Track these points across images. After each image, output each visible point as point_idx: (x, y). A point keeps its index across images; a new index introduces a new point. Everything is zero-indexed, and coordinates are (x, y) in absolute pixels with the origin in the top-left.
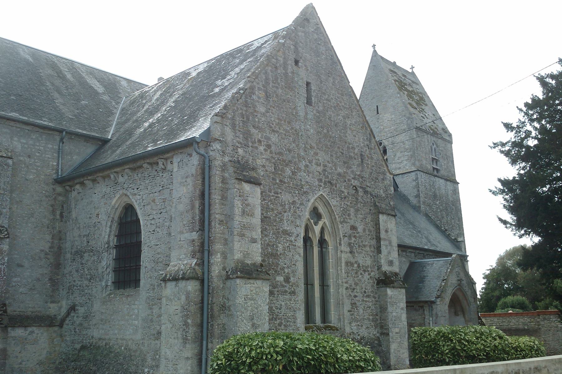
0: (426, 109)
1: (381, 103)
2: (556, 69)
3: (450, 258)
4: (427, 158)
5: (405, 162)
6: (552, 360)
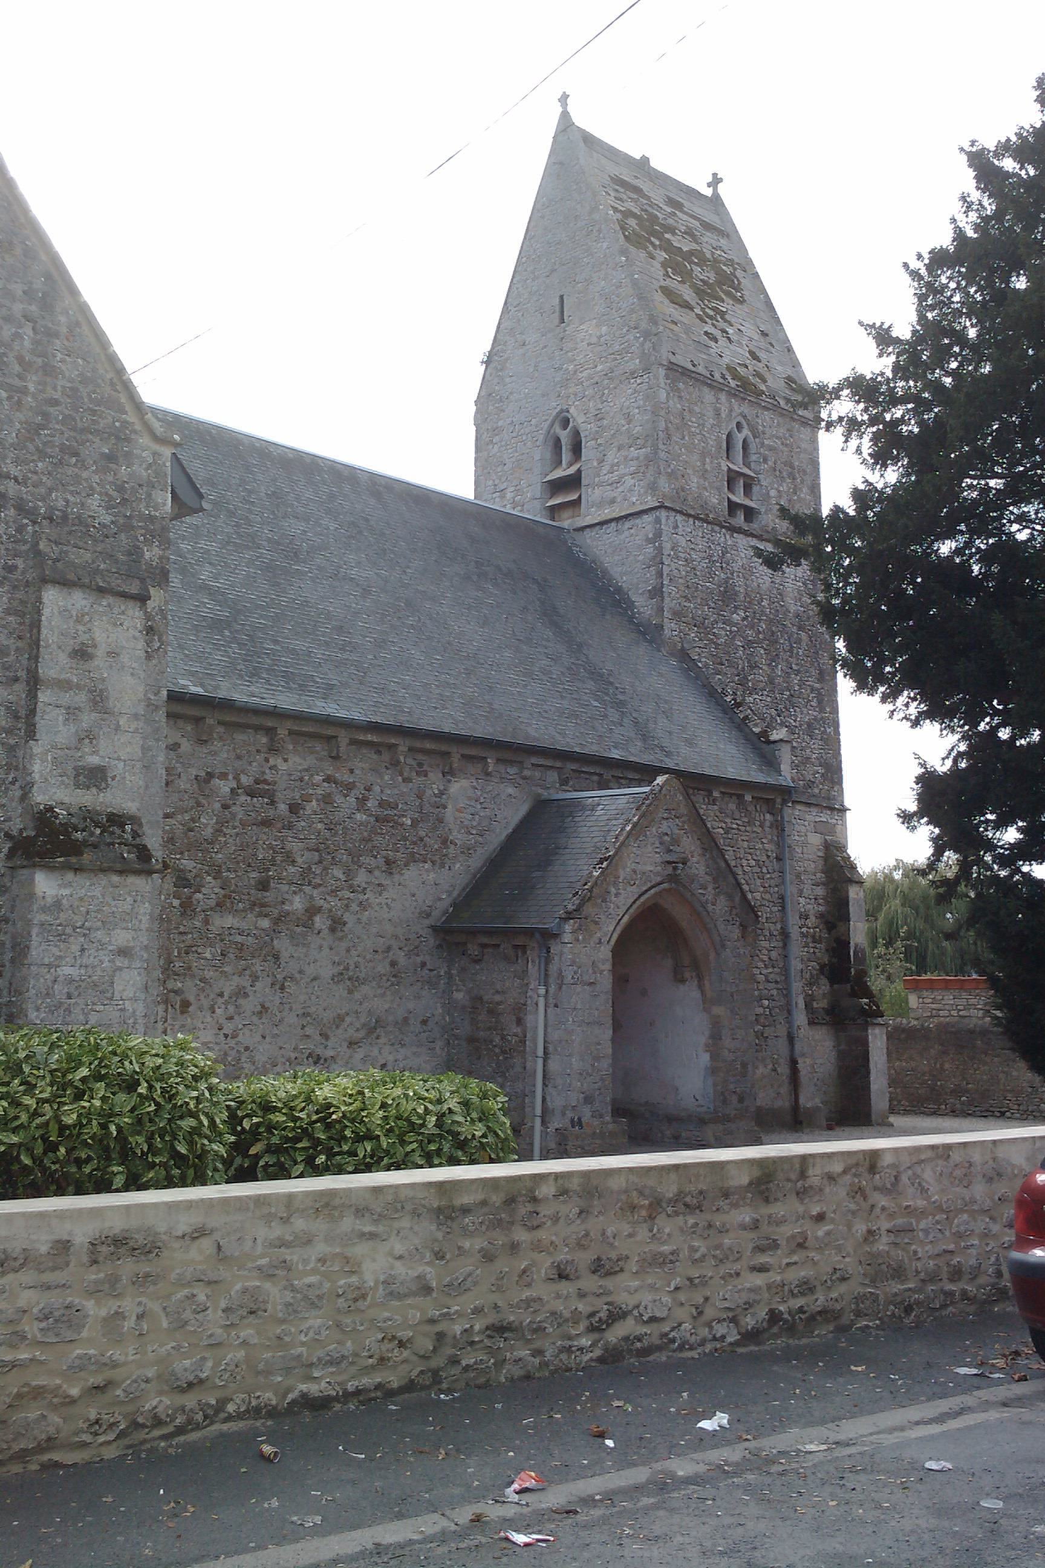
0: (736, 313)
1: (574, 287)
2: (1031, 117)
3: (647, 789)
4: (706, 471)
5: (629, 481)
6: (260, 1201)
